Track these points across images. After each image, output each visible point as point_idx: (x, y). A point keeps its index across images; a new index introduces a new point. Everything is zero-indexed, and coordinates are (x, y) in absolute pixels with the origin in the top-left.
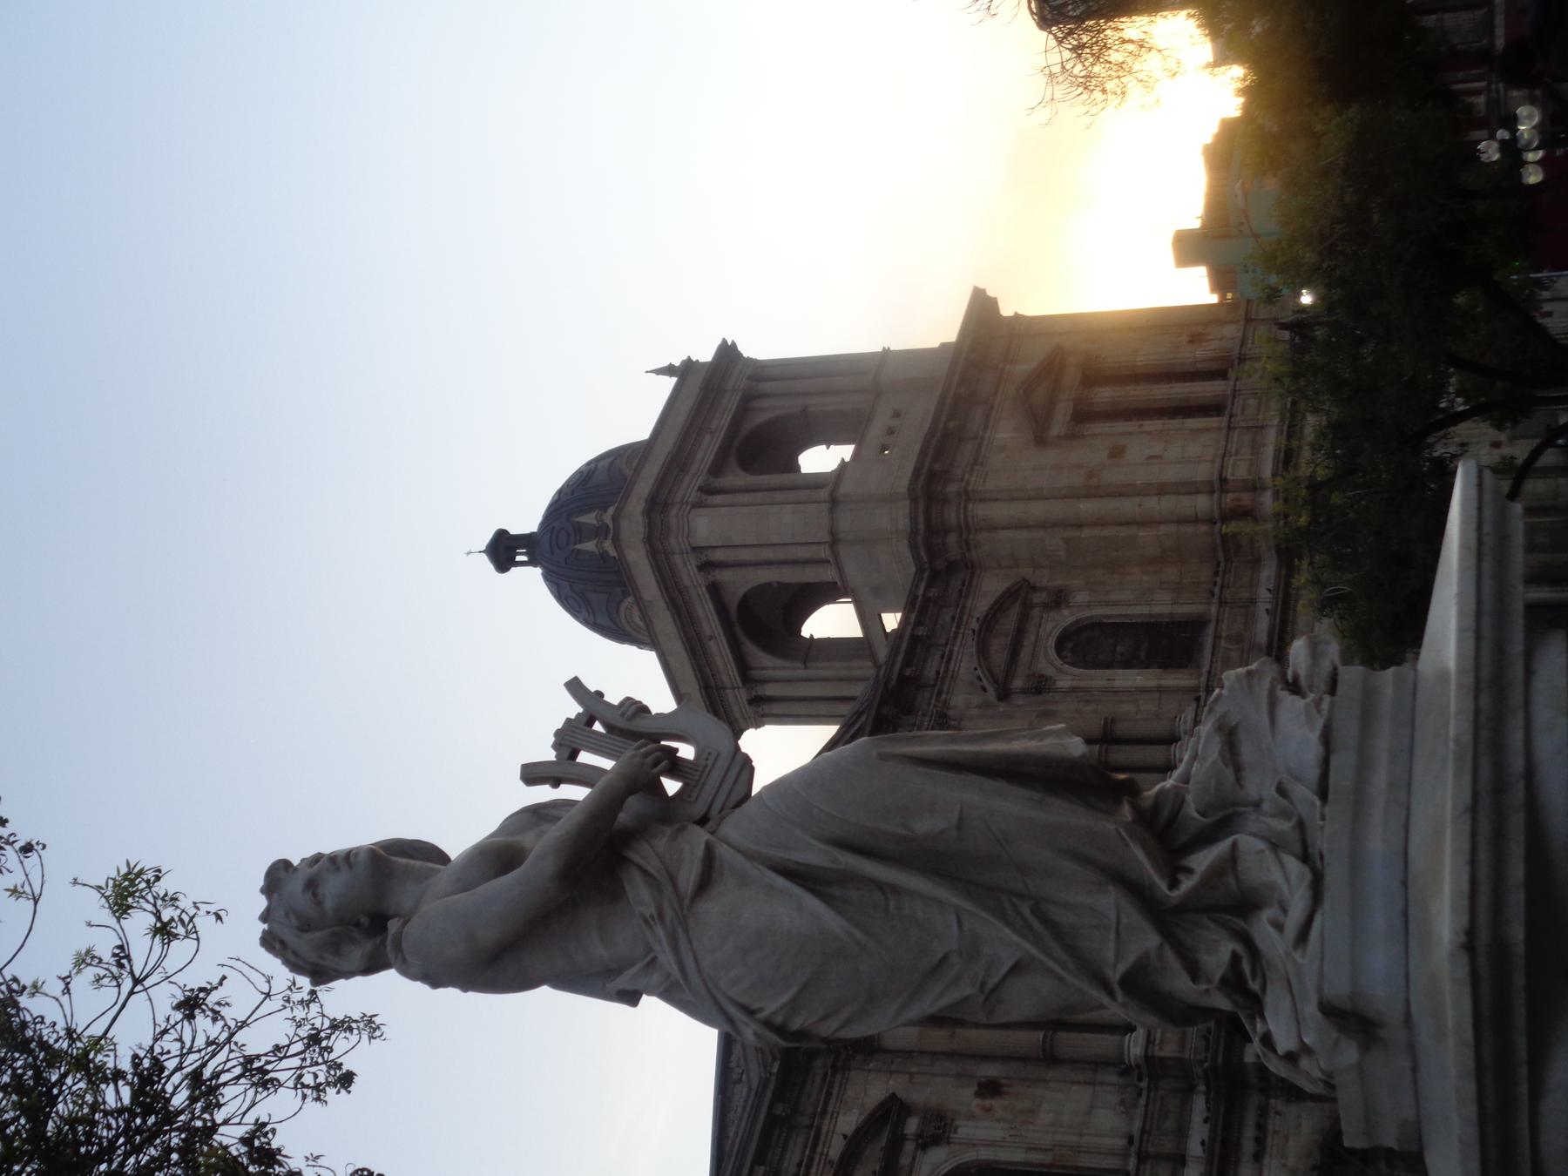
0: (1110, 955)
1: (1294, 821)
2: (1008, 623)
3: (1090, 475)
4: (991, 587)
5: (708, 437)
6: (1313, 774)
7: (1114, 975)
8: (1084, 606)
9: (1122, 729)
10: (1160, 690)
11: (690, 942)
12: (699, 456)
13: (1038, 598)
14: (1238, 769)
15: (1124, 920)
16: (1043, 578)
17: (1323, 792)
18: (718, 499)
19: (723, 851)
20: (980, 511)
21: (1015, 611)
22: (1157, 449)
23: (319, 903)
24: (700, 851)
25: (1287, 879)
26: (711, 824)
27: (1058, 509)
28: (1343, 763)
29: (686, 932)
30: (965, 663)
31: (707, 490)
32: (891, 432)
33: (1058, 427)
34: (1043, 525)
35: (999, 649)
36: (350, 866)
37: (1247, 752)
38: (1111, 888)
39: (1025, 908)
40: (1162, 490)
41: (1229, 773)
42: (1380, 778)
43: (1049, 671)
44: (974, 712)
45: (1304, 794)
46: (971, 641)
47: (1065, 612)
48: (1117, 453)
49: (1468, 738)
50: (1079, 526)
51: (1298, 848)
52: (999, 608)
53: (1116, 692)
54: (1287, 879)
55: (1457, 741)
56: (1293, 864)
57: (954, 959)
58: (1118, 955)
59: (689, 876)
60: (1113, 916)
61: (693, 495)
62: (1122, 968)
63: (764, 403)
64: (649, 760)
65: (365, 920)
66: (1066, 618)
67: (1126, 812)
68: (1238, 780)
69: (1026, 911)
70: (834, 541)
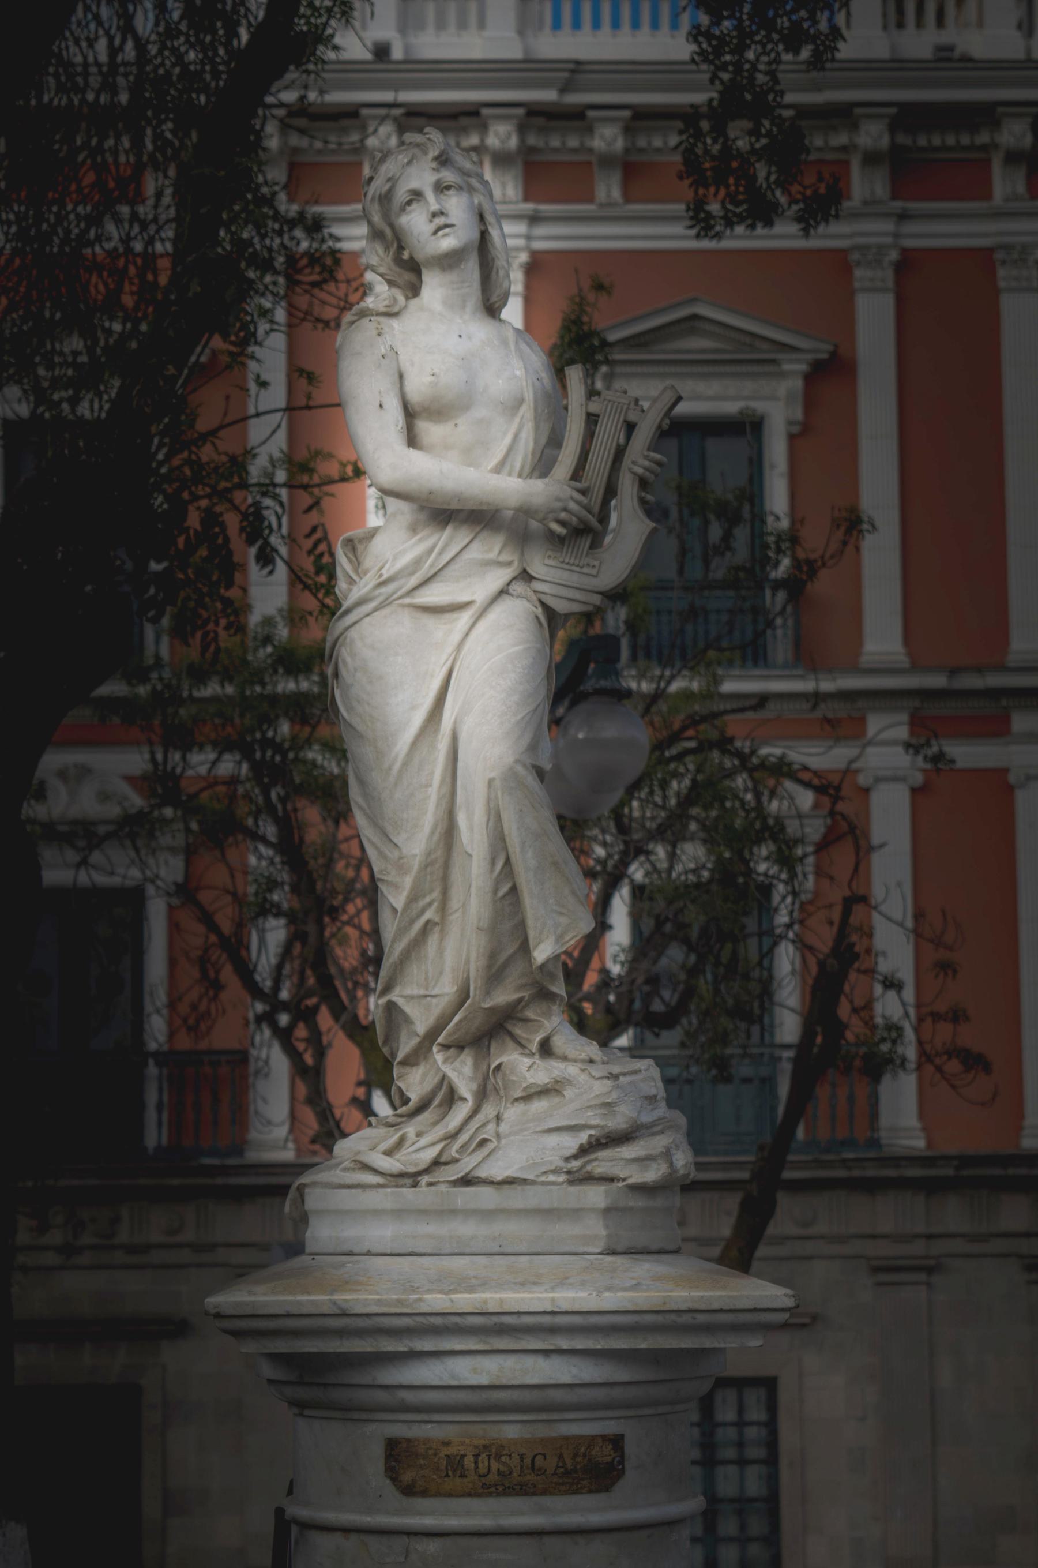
0: (408, 991)
1: (457, 1156)
6: (482, 1173)
7: (395, 996)
11: (368, 615)
14: (527, 1098)
15: (434, 1001)
17: (467, 1181)
19: (465, 618)
23: (403, 209)
24: (464, 598)
25: (417, 1151)
26: (518, 587)
28: (485, 1197)
29: (376, 609)
36: (435, 233)
37: (539, 1106)
38: (455, 988)
39: (428, 915)
41: (519, 1094)
42: (466, 1229)
45: (468, 1164)
49: (424, 1308)
51: (443, 1159)
54: (417, 1151)
55: (420, 1300)
56: (428, 1156)
57: (396, 853)
58: (411, 998)
59: (433, 595)
60: (434, 993)
62: (400, 1002)
64: (563, 515)
65: (406, 256)
67: (503, 997)
68: (516, 1100)
69: (428, 915)
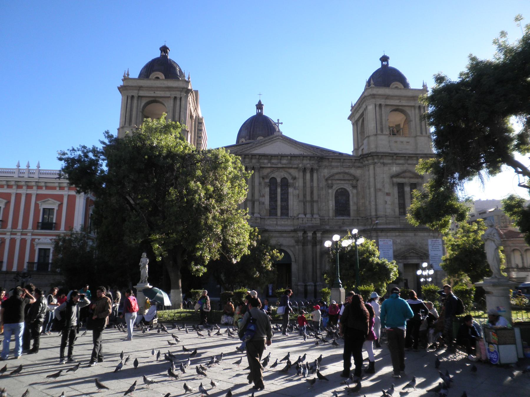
2: (347, 177)
3: (380, 190)
4: (358, 172)
5: (398, 101)
8: (352, 192)
9: (315, 205)
10: (329, 210)
12: (392, 101)
13: (354, 182)
16: (359, 183)
18: (377, 108)
20: (371, 167)
21: (350, 178)
22: (389, 202)
27: (372, 184)
30: (335, 171)
31: (380, 105)
32: (402, 142)
33: (395, 180)
34: (369, 182)
35: (341, 176)
40: (376, 205)
43: (334, 187)
44: (322, 174)
46: (342, 171)
47: (351, 188)
48: (388, 194)
50: (369, 189)
52: (351, 175)
53: (328, 201)
61: (378, 103)
63: (413, 112)
66: (349, 189)
70: (369, 137)
